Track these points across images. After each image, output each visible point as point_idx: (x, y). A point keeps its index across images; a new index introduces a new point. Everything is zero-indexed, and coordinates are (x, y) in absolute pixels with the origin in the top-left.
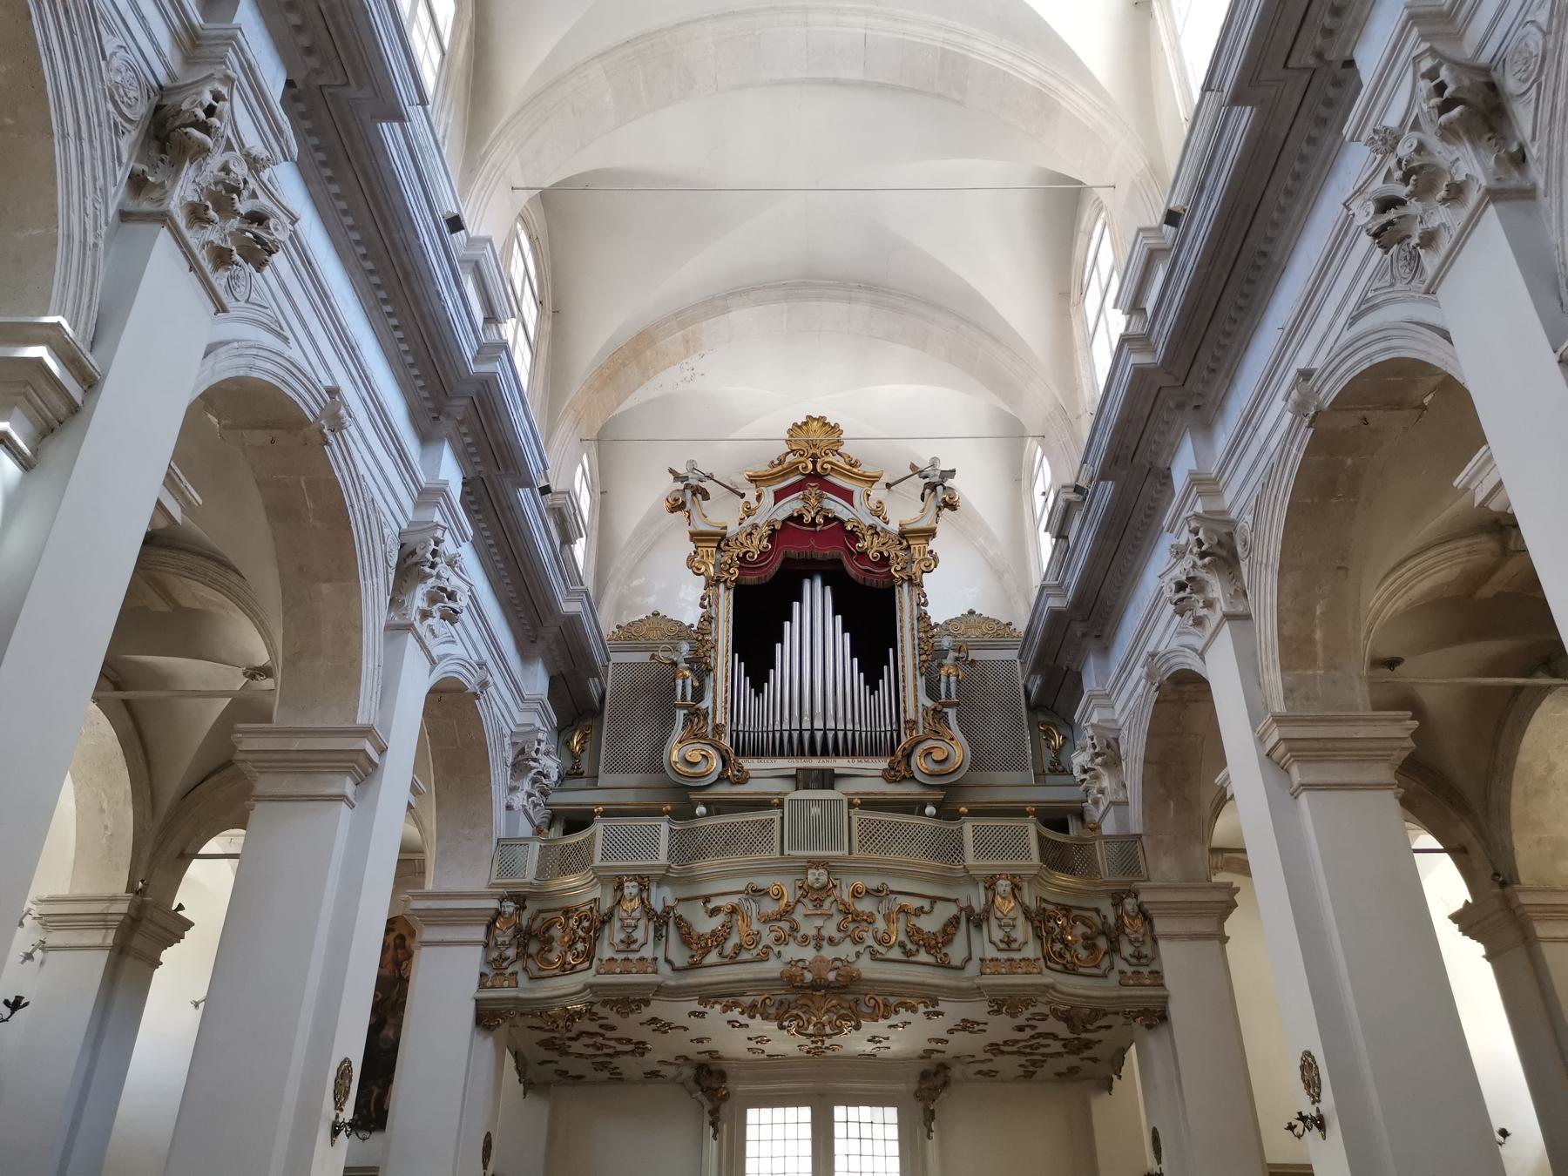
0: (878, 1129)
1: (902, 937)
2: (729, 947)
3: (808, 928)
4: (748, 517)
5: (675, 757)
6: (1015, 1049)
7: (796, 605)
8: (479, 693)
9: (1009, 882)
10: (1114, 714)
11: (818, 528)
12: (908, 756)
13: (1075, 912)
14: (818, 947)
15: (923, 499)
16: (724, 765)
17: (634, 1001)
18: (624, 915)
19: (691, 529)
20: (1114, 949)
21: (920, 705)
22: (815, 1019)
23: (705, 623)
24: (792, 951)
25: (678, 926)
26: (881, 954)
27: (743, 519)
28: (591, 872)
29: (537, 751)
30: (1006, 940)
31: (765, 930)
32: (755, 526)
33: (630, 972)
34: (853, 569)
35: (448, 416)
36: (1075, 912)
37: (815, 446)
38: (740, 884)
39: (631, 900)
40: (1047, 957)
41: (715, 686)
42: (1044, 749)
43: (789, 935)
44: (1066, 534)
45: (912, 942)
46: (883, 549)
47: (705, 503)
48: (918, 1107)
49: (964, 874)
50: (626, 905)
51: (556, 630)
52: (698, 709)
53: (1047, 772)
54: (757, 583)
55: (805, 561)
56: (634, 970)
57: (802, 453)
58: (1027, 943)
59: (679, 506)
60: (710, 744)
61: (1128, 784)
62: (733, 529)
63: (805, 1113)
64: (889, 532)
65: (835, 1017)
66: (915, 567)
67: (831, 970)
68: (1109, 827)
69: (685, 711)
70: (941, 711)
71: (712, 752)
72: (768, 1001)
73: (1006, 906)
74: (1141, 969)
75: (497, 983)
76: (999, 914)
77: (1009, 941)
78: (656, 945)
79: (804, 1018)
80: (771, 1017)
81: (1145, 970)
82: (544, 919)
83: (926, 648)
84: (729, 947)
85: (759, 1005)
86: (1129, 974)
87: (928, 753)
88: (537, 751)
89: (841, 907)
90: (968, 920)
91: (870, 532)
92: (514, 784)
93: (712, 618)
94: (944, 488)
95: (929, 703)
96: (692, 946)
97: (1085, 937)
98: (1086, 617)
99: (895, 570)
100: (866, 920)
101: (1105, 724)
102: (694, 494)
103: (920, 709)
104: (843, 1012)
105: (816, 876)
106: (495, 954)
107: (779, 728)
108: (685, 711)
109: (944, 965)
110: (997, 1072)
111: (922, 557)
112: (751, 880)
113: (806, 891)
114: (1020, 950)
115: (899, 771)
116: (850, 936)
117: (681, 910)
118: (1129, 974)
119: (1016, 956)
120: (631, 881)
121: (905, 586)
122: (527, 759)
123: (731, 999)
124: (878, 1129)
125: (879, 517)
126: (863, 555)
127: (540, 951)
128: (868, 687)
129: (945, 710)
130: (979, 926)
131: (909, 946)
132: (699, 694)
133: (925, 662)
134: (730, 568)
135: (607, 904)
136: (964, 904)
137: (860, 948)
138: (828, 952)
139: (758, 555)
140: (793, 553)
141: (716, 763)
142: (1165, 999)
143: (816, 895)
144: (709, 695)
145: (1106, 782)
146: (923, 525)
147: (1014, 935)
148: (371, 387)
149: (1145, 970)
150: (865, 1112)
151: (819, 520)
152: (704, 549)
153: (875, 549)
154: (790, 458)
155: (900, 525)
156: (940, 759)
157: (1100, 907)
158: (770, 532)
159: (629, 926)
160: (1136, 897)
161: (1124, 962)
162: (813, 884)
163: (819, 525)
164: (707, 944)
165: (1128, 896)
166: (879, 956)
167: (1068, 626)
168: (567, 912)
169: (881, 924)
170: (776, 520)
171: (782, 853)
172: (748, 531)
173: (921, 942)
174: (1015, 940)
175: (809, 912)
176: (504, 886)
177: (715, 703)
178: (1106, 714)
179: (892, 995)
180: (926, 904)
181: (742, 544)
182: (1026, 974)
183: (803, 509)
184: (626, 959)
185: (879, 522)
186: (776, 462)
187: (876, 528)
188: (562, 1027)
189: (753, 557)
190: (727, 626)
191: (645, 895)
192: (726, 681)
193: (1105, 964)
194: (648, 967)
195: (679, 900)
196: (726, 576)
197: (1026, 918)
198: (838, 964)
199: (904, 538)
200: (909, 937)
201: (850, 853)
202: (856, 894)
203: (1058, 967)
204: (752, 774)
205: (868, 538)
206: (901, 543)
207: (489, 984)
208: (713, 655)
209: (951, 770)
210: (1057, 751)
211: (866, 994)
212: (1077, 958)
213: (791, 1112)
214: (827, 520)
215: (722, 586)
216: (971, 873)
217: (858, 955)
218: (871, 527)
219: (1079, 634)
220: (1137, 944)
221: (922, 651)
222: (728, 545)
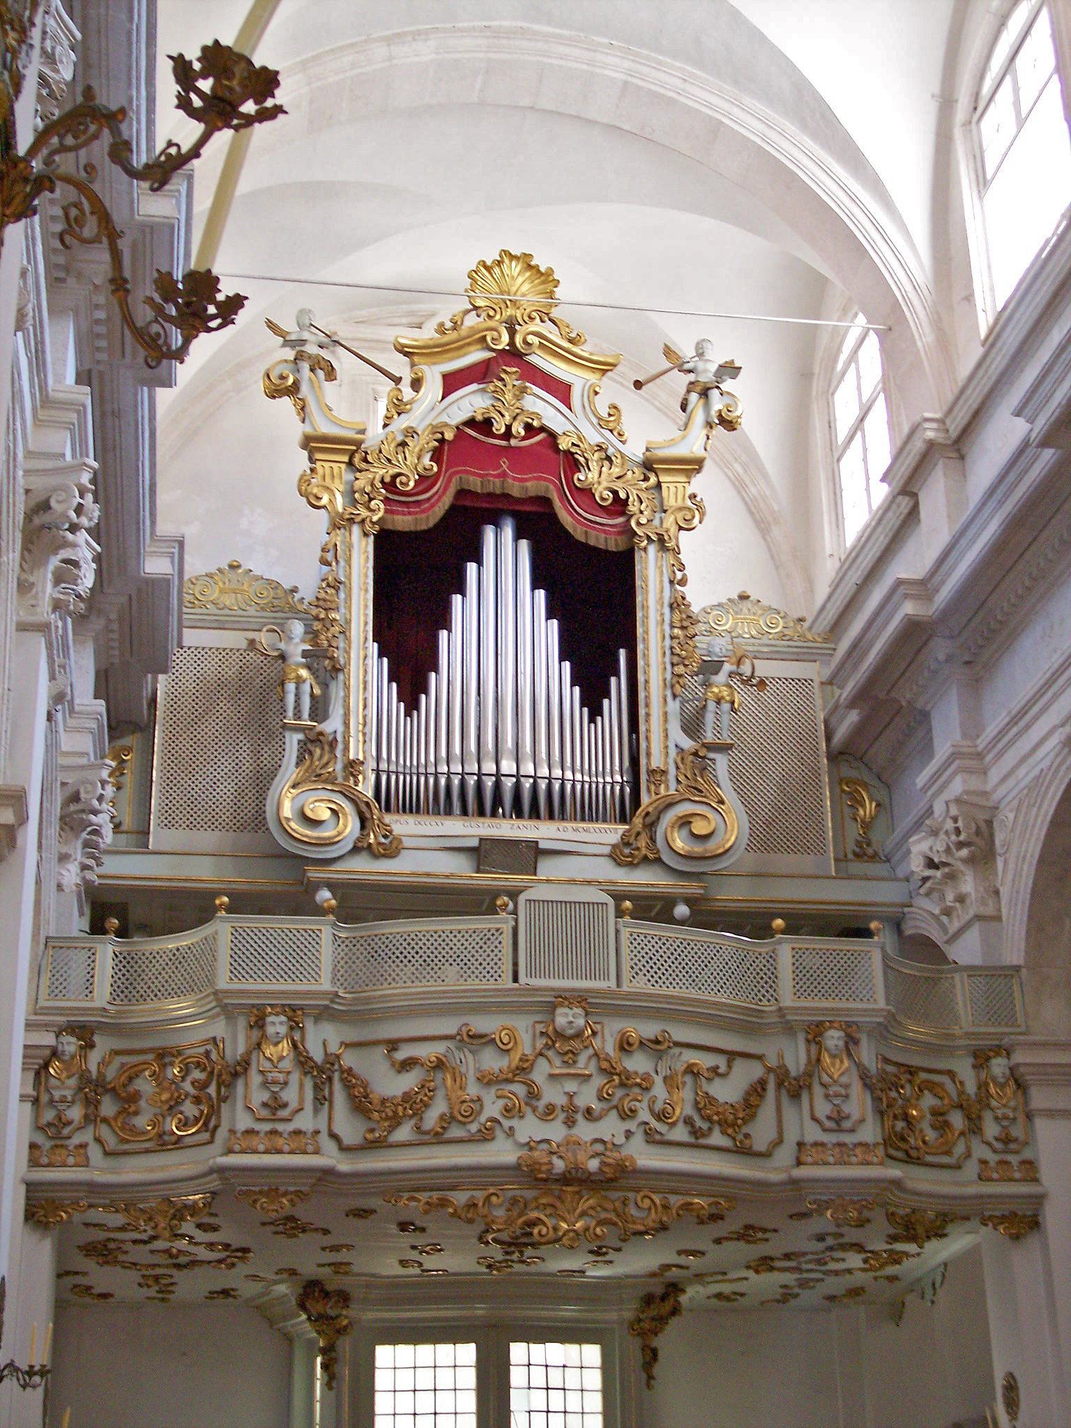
0: (572, 1378)
1: (689, 1111)
2: (431, 1118)
3: (553, 1095)
4: (399, 414)
5: (287, 811)
6: (793, 1264)
7: (472, 568)
9: (842, 1034)
10: (985, 782)
11: (513, 442)
12: (651, 826)
13: (923, 1076)
14: (570, 1123)
15: (684, 407)
16: (363, 827)
18: (267, 1065)
19: (308, 430)
20: (974, 1127)
22: (565, 1226)
23: (331, 591)
24: (530, 1128)
25: (348, 1086)
26: (661, 1134)
29: (101, 798)
30: (835, 1115)
33: (280, 1152)
35: (79, 276)
36: (923, 1076)
38: (449, 1026)
39: (276, 1044)
40: (887, 1142)
41: (347, 696)
42: (849, 823)
45: (702, 1117)
46: (618, 486)
47: (327, 385)
48: (633, 1346)
49: (778, 1020)
50: (269, 1050)
51: (124, 599)
52: (321, 734)
53: (850, 856)
54: (413, 528)
55: (490, 495)
57: (492, 313)
58: (863, 1120)
61: (1005, 892)
62: (375, 434)
63: (467, 1353)
65: (593, 1223)
66: (669, 522)
67: (593, 1157)
68: (967, 950)
69: (301, 736)
70: (704, 758)
71: (348, 807)
72: (494, 1199)
73: (838, 1069)
74: (1010, 1158)
76: (826, 1079)
77: (838, 1119)
78: (316, 1111)
79: (549, 1225)
81: (1014, 1159)
82: (123, 1065)
84: (431, 1118)
85: (480, 1204)
87: (685, 822)
88: (101, 798)
89: (605, 1065)
90: (780, 1085)
91: (597, 455)
92: (64, 850)
93: (340, 583)
95: (688, 744)
96: (371, 1116)
97: (935, 1113)
98: (956, 632)
100: (639, 1085)
101: (975, 799)
102: (312, 370)
103: (673, 752)
104: (604, 1215)
106: (49, 1115)
108: (301, 736)
109: (743, 1151)
110: (742, 1295)
111: (680, 503)
112: (466, 1019)
114: (852, 1131)
115: (638, 849)
116: (616, 1107)
117: (349, 1060)
118: (992, 1164)
119: (848, 1139)
120: (277, 1014)
121: (652, 549)
122: (83, 811)
123: (436, 1195)
124: (572, 1378)
125: (611, 431)
126: (586, 493)
128: (585, 710)
130: (795, 1096)
131: (699, 1123)
132: (320, 709)
133: (680, 676)
134: (371, 499)
136: (772, 1062)
137: (631, 1125)
138: (585, 1131)
139: (416, 481)
140: (475, 483)
141: (351, 825)
142: (1039, 1199)
144: (336, 712)
145: (968, 884)
146: (681, 451)
147: (846, 1109)
148: (34, 251)
149: (1014, 1159)
150: (555, 1352)
151: (518, 429)
152: (327, 465)
153: (605, 484)
154: (471, 321)
155: (648, 450)
156: (704, 832)
157: (956, 1069)
158: (436, 444)
159: (275, 1082)
160: (1008, 1055)
161: (984, 1146)
163: (516, 438)
164: (395, 1113)
165: (998, 1054)
166: (657, 1137)
167: (925, 643)
168: (163, 1056)
169: (659, 1090)
170: (446, 425)
171: (516, 980)
172: (400, 438)
173: (715, 1118)
174: (848, 1117)
175: (557, 1071)
176: (60, 1011)
177: (346, 724)
178: (975, 783)
179: (675, 1192)
180: (721, 1061)
181: (389, 460)
182: (862, 1164)
183: (492, 408)
184: (274, 1132)
186: (449, 325)
187: (606, 450)
188: (165, 1229)
189: (407, 485)
190: (366, 600)
193: (959, 1149)
194: (307, 1144)
195: (347, 1045)
196: (364, 513)
197: (865, 1085)
198: (599, 1147)
199: (650, 469)
200: (699, 1110)
201: (618, 986)
202: (625, 1046)
203: (900, 1154)
204: (407, 842)
205: (593, 465)
206: (646, 479)
207: (45, 1160)
208: (342, 645)
209: (720, 851)
210: (867, 826)
211: (638, 1192)
212: (924, 1142)
213: (445, 1351)
214: (528, 427)
215: (356, 529)
216: (789, 1017)
217: (628, 1134)
218: (600, 448)
219: (941, 657)
220: (1005, 1123)
221: (676, 659)
222: (365, 460)
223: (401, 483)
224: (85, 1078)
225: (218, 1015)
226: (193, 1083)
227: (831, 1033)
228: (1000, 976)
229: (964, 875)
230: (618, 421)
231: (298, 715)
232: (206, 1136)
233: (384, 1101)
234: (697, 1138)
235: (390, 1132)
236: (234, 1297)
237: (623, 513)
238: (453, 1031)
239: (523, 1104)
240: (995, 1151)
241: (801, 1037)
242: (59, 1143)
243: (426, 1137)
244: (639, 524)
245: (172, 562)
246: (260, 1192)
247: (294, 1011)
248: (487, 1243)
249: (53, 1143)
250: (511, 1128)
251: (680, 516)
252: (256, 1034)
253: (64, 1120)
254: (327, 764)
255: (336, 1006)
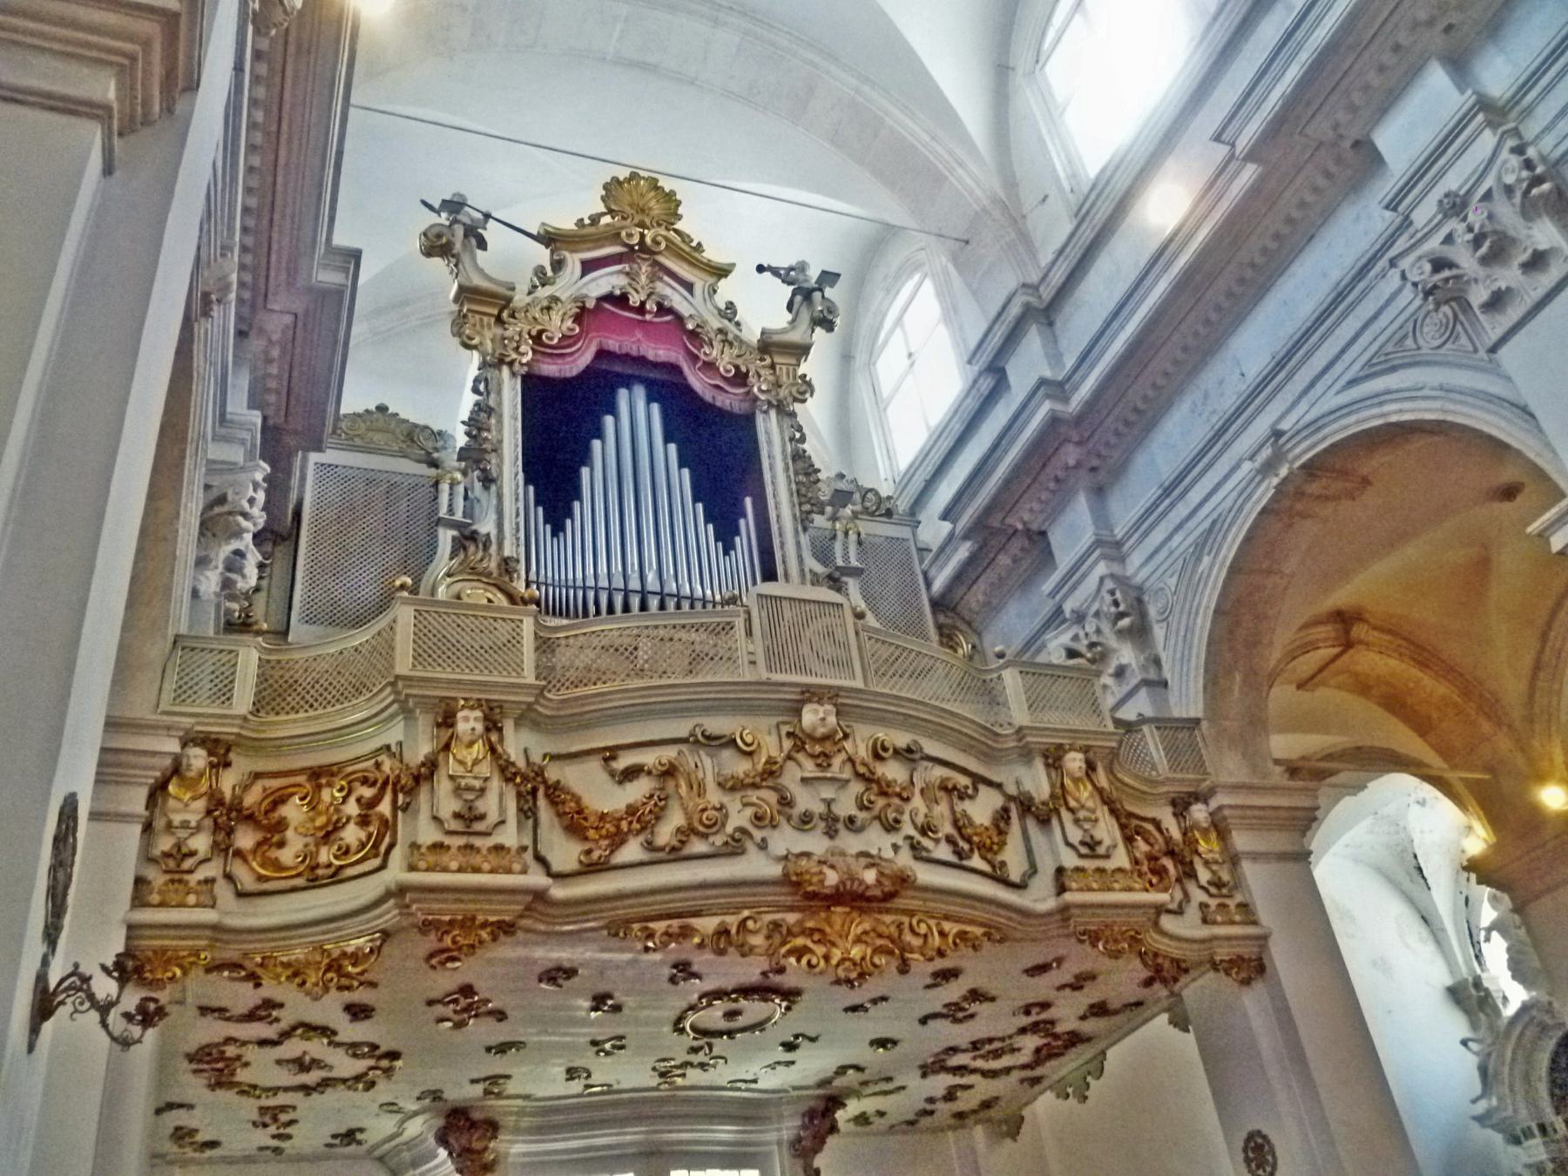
2: (665, 834)
3: (806, 801)
4: (543, 285)
8: (214, 297)
11: (648, 317)
14: (831, 833)
15: (790, 307)
17: (484, 925)
18: (459, 770)
21: (807, 570)
23: (483, 415)
25: (553, 802)
27: (535, 287)
28: (389, 690)
31: (733, 803)
32: (555, 299)
34: (697, 381)
36: (1135, 822)
37: (643, 211)
38: (681, 728)
39: (471, 744)
43: (779, 812)
44: (1002, 364)
46: (739, 362)
47: (479, 253)
50: (458, 750)
51: (288, 319)
52: (475, 532)
54: (557, 375)
56: (486, 866)
59: (442, 246)
60: (495, 585)
61: (1163, 656)
64: (748, 346)
65: (869, 951)
66: (783, 393)
74: (1227, 901)
75: (174, 898)
77: (1092, 845)
78: (520, 824)
80: (758, 950)
83: (810, 495)
84: (665, 834)
85: (734, 931)
86: (1213, 908)
92: (203, 553)
94: (823, 296)
99: (760, 390)
102: (466, 236)
104: (879, 942)
105: (812, 716)
106: (165, 844)
107: (593, 584)
108: (455, 533)
113: (800, 741)
114: (1107, 856)
118: (1213, 908)
120: (472, 708)
121: (773, 413)
123: (675, 923)
125: (730, 320)
126: (710, 366)
127: (259, 844)
128: (720, 545)
129: (845, 579)
130: (1044, 822)
133: (809, 513)
135: (421, 749)
137: (898, 838)
138: (851, 843)
140: (613, 344)
143: (821, 747)
149: (1232, 903)
152: (478, 317)
154: (606, 220)
155: (763, 333)
159: (469, 789)
162: (814, 729)
164: (618, 827)
166: (924, 854)
168: (318, 775)
172: (545, 303)
173: (976, 839)
179: (947, 918)
181: (535, 319)
185: (731, 327)
186: (587, 221)
187: (726, 334)
188: (316, 984)
191: (494, 737)
192: (517, 500)
195: (555, 757)
196: (514, 356)
206: (762, 360)
207: (155, 898)
208: (493, 461)
214: (660, 306)
215: (505, 370)
216: (1029, 739)
218: (720, 331)
219: (1072, 462)
221: (803, 500)
222: (512, 316)
223: (547, 338)
224: (215, 800)
225: (392, 717)
226: (359, 800)
227: (1072, 755)
228: (1183, 728)
229: (1115, 651)
230: (735, 313)
231: (451, 510)
232: (376, 862)
233: (602, 817)
234: (961, 858)
235: (612, 852)
236: (359, 1143)
237: (744, 384)
238: (684, 733)
239: (775, 813)
240: (1211, 895)
241: (1039, 764)
242: (177, 877)
243: (661, 855)
244: (760, 390)
245: (347, 278)
246: (451, 923)
247: (491, 709)
248: (682, 1031)
249: (168, 877)
250: (763, 840)
251: (794, 390)
252: (445, 734)
253: (184, 850)
254: (482, 560)
255: (540, 709)
